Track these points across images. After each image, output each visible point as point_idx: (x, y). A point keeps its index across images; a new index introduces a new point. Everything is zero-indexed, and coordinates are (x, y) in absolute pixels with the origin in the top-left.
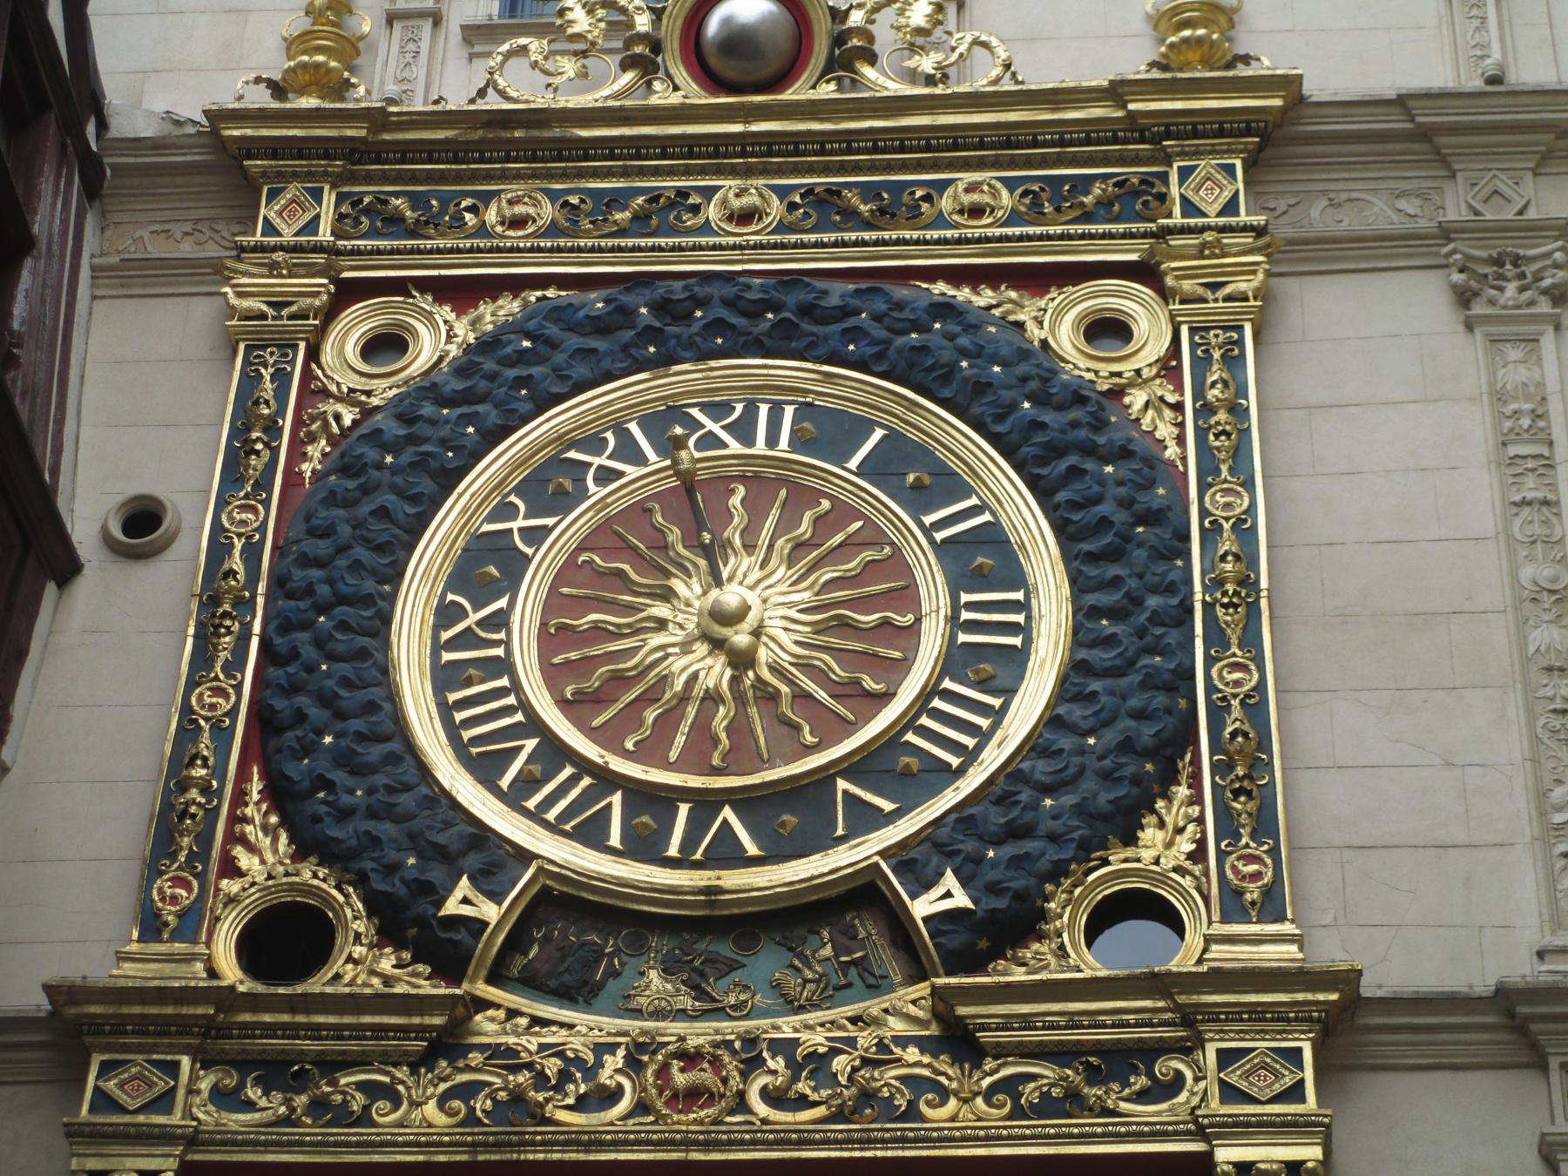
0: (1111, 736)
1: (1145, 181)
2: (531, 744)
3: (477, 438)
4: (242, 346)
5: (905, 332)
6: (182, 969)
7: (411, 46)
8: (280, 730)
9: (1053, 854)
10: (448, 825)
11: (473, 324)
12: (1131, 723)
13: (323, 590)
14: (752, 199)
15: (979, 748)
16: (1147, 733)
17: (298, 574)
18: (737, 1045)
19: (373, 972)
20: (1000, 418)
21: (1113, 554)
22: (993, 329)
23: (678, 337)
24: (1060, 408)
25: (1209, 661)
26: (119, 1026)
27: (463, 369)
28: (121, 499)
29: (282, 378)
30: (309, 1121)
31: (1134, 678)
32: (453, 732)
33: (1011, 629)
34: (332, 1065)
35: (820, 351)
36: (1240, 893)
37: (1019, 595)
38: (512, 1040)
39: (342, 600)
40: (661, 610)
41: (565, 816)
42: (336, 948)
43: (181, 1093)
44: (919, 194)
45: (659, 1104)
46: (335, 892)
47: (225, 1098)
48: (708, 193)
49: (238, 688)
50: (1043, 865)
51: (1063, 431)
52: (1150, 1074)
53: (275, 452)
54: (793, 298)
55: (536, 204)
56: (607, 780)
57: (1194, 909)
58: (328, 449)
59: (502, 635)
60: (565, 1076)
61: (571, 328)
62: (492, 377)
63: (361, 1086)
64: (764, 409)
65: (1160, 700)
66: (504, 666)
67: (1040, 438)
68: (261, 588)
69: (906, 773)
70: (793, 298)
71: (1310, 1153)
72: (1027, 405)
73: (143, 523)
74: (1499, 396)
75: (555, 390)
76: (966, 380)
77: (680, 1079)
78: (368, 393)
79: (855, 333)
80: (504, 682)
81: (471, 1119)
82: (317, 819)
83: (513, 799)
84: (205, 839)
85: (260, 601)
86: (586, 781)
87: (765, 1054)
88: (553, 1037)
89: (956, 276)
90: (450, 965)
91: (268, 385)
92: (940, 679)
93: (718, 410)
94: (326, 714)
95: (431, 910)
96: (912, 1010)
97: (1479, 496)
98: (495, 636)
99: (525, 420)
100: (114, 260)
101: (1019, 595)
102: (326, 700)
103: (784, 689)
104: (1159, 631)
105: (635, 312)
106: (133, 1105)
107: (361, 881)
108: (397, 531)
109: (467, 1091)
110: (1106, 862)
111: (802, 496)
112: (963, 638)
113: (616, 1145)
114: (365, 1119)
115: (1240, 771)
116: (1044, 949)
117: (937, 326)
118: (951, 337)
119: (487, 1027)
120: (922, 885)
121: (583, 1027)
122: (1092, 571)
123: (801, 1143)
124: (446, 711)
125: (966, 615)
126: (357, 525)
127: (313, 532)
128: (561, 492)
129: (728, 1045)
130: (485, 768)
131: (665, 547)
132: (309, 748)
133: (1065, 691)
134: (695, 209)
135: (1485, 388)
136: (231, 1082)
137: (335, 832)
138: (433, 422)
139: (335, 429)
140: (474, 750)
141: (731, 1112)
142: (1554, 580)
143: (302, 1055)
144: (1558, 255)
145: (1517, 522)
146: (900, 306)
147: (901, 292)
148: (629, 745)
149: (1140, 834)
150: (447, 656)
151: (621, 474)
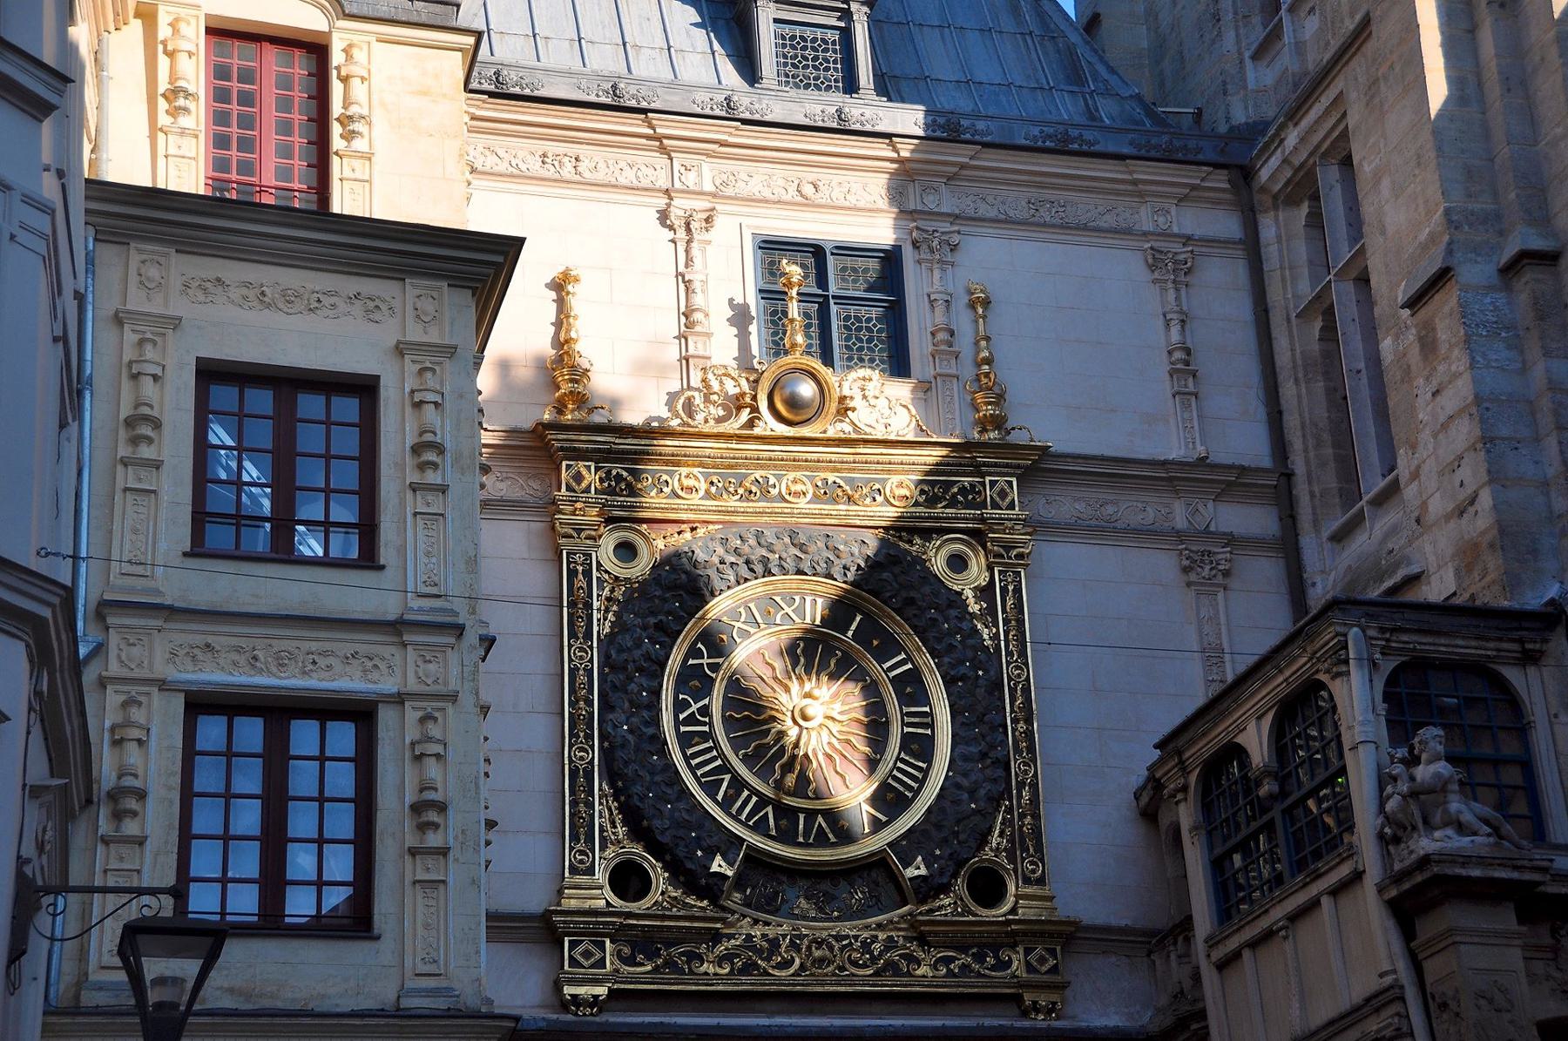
1: (972, 485)
2: (727, 777)
32: (693, 770)
41: (749, 817)
48: (779, 478)
55: (697, 478)
56: (763, 801)
63: (682, 954)
64: (808, 599)
77: (817, 953)
83: (725, 805)
86: (754, 799)
111: (829, 651)
120: (907, 865)
124: (687, 759)
130: (711, 789)
150: (683, 729)
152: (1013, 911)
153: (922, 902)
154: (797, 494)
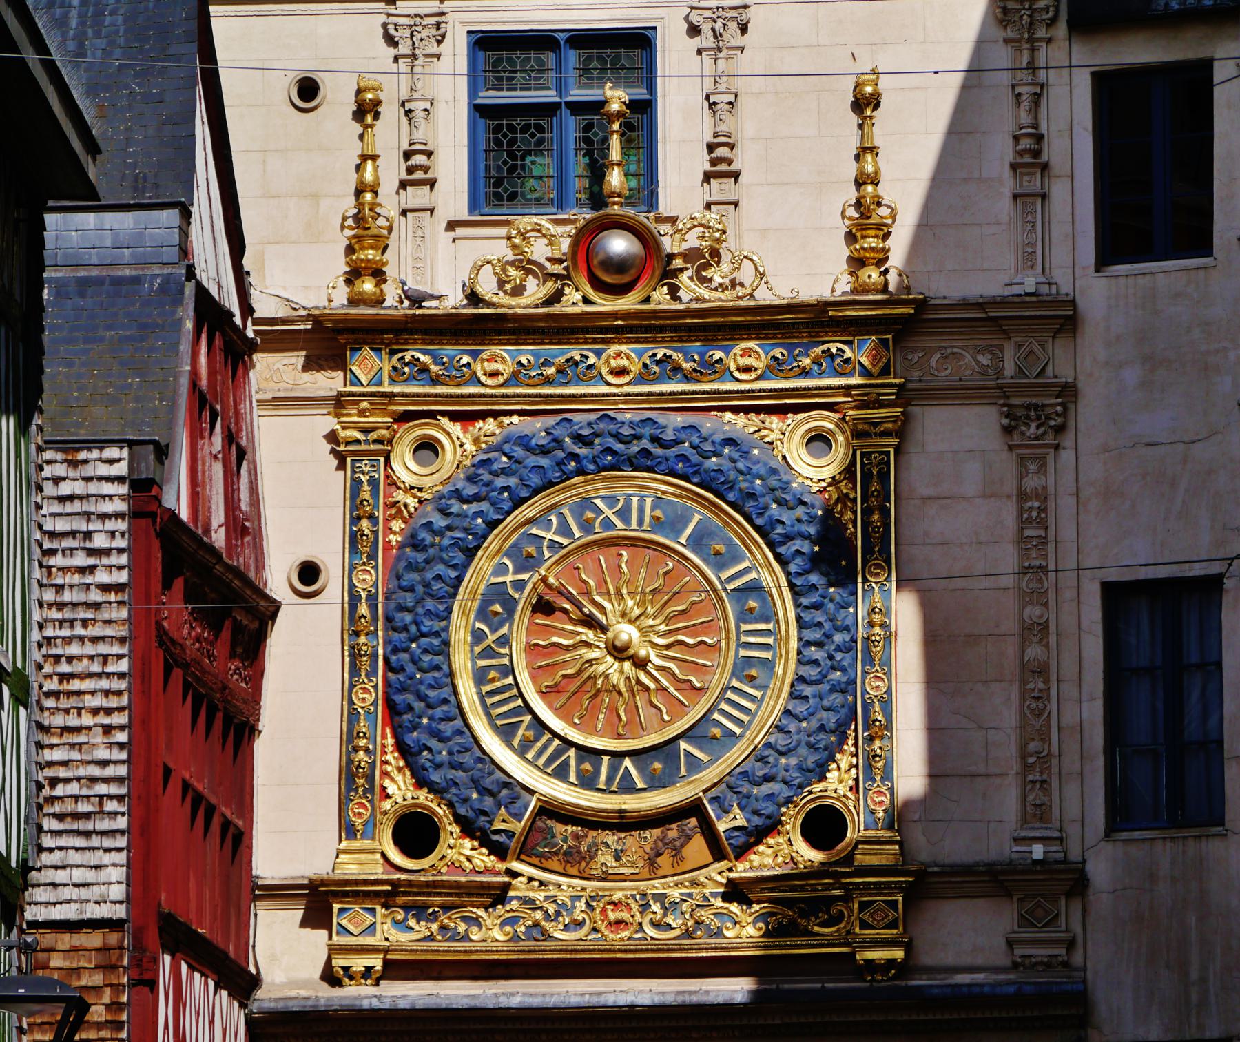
0: (814, 724)
3: (484, 526)
4: (349, 460)
5: (709, 458)
6: (370, 856)
7: (419, 233)
8: (400, 714)
9: (787, 792)
10: (490, 774)
11: (476, 441)
12: (824, 714)
13: (413, 629)
14: (624, 362)
15: (750, 722)
16: (831, 719)
17: (399, 616)
18: (638, 897)
19: (460, 854)
20: (760, 515)
21: (816, 607)
22: (756, 452)
23: (587, 457)
24: (791, 509)
25: (865, 673)
26: (346, 894)
27: (471, 479)
28: (298, 563)
29: (373, 483)
30: (439, 938)
31: (825, 687)
33: (766, 647)
34: (446, 908)
35: (663, 467)
36: (873, 813)
37: (770, 626)
38: (531, 894)
39: (423, 635)
40: (589, 635)
42: (441, 839)
43: (378, 926)
44: (716, 357)
45: (603, 929)
46: (437, 809)
47: (401, 925)
49: (376, 687)
50: (781, 800)
51: (793, 526)
52: (828, 913)
53: (376, 533)
54: (647, 431)
57: (853, 817)
58: (403, 526)
59: (505, 651)
60: (558, 913)
61: (527, 448)
62: (487, 484)
64: (635, 500)
65: (836, 699)
66: (509, 670)
67: (779, 530)
68: (380, 624)
69: (714, 737)
70: (647, 431)
71: (899, 954)
72: (774, 506)
73: (309, 572)
74: (1023, 496)
75: (524, 494)
76: (740, 490)
77: (612, 916)
78: (420, 490)
79: (683, 457)
80: (510, 680)
81: (515, 938)
82: (426, 770)
83: (521, 752)
84: (370, 778)
85: (380, 633)
87: (651, 902)
88: (552, 891)
89: (735, 410)
90: (499, 851)
91: (366, 487)
92: (730, 679)
93: (611, 500)
94: (422, 704)
95: (488, 825)
96: (719, 878)
97: (1007, 557)
98: (502, 651)
99: (509, 513)
100: (269, 396)
101: (770, 626)
102: (422, 697)
103: (652, 686)
104: (838, 656)
105: (563, 441)
106: (356, 932)
107: (450, 805)
108: (447, 588)
109: (512, 921)
110: (810, 792)
112: (743, 652)
113: (584, 951)
114: (466, 938)
115: (877, 743)
116: (781, 841)
117: (726, 451)
118: (734, 461)
119: (520, 888)
121: (566, 887)
122: (807, 616)
123: (669, 950)
125: (744, 639)
126: (427, 585)
127: (401, 588)
128: (529, 556)
129: (633, 896)
130: (506, 733)
131: (588, 594)
132: (415, 727)
133: (793, 696)
134: (591, 367)
135: (1015, 492)
136: (400, 917)
137: (436, 777)
138: (458, 515)
139: (405, 513)
140: (499, 723)
141: (636, 932)
142: (1041, 617)
143: (433, 905)
144: (1059, 409)
145: (1026, 579)
146: (706, 439)
147: (707, 423)
148: (576, 721)
149: (828, 775)
151: (561, 546)
152: (849, 859)
153: (741, 852)
154: (621, 372)
